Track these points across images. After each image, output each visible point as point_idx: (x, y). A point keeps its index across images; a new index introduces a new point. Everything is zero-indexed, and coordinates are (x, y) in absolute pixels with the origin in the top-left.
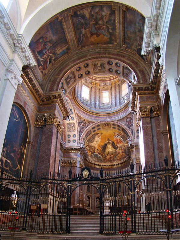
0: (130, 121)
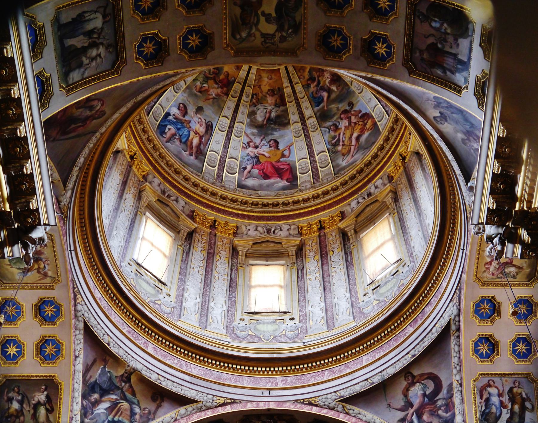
0: (432, 397)
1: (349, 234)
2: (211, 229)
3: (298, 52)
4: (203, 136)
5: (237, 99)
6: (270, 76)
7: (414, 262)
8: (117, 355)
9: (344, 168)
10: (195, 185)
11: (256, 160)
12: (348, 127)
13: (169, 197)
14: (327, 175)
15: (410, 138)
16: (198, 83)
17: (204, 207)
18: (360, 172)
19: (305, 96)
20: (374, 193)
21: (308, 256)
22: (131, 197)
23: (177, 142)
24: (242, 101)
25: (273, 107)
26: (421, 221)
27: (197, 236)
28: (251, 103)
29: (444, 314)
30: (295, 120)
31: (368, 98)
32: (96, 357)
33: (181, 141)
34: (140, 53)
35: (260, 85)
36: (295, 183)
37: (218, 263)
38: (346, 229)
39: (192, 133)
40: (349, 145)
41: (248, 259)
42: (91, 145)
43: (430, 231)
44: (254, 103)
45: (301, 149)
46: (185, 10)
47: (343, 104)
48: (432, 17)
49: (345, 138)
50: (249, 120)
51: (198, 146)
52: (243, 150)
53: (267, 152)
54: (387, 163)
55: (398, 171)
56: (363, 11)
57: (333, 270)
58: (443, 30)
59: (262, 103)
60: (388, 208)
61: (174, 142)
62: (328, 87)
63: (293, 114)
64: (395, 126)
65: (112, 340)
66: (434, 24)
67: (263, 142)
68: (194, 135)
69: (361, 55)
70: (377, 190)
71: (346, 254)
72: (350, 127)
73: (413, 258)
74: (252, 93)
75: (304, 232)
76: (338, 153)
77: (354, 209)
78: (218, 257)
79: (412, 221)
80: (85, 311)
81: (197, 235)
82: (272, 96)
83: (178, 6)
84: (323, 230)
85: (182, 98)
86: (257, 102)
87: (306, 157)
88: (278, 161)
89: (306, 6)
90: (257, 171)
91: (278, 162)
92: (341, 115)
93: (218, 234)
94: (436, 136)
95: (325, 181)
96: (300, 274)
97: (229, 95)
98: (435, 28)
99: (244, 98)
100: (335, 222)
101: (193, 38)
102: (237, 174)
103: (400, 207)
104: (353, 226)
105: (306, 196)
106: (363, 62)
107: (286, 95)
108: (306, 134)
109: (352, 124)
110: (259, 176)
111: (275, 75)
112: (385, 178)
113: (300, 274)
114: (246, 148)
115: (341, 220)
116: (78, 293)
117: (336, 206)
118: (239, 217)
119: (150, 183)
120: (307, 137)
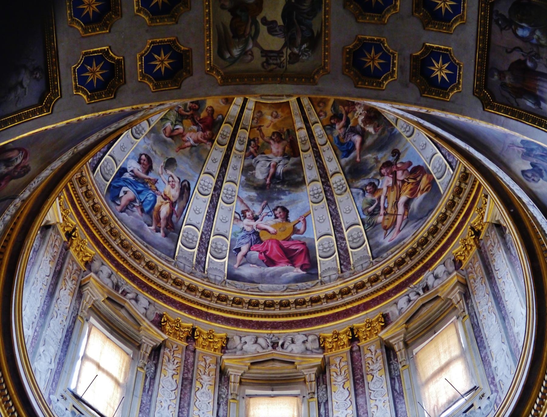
1: (396, 348)
2: (187, 342)
3: (316, 77)
5: (226, 146)
6: (274, 113)
7: (497, 391)
9: (386, 249)
10: (164, 275)
13: (124, 293)
14: (362, 258)
15: (486, 203)
16: (168, 124)
17: (177, 309)
18: (412, 254)
19: (327, 142)
20: (433, 287)
21: (334, 383)
22: (67, 295)
23: (138, 212)
24: (233, 150)
25: (279, 158)
26: (505, 328)
27: (166, 353)
28: (247, 153)
30: (313, 178)
33: (142, 211)
34: (82, 80)
35: (260, 126)
36: (313, 272)
37: (198, 394)
38: (391, 341)
39: (159, 199)
40: (394, 215)
41: (243, 387)
42: (8, 218)
43: (520, 344)
44: (251, 153)
45: (321, 221)
46: (150, 16)
47: (384, 153)
48: (517, 22)
50: (243, 178)
51: (169, 218)
52: (235, 222)
53: (272, 226)
54: (453, 241)
55: (468, 252)
56: (413, 14)
57: (373, 403)
58: (534, 41)
59: (264, 153)
60: (455, 308)
61: (133, 211)
62: (361, 128)
63: (310, 168)
64: (463, 185)
66: (520, 32)
67: (266, 211)
68: (163, 200)
69: (410, 81)
70: (437, 281)
71: (392, 379)
72: (395, 187)
73: (495, 386)
74: (249, 138)
75: (328, 345)
76: (377, 226)
77: (403, 311)
78: (198, 385)
79: (492, 328)
81: (167, 351)
82: (279, 142)
83: (139, 11)
84: (356, 342)
85: (144, 146)
86: (255, 151)
87: (329, 232)
88: (288, 239)
89: (327, 9)
90: (257, 254)
91: (288, 240)
92: (381, 169)
93: (199, 349)
94: (526, 199)
95: (359, 268)
96: (322, 411)
97: (214, 141)
98: (522, 38)
99: (237, 145)
100: (375, 330)
101: (160, 58)
102: (226, 259)
103: (472, 306)
104: (403, 335)
105: (330, 292)
106: (414, 91)
108: (329, 197)
109: (398, 183)
110: (260, 262)
111: (283, 111)
112: (449, 262)
113: (322, 411)
114: (240, 220)
115: (383, 328)
117: (375, 306)
118: (230, 323)
119: (96, 273)
120: (331, 202)
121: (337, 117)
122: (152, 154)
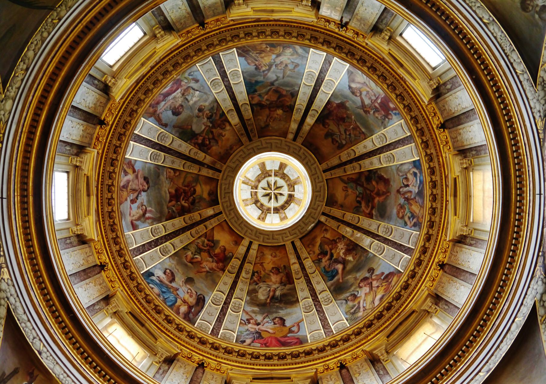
4: (193, 307)
5: (235, 275)
6: (274, 254)
8: (51, 371)
11: (257, 335)
12: (369, 292)
16: (189, 253)
24: (241, 277)
25: (277, 285)
28: (252, 281)
29: (526, 299)
31: (391, 255)
32: (18, 366)
35: (262, 263)
38: (374, 352)
44: (255, 281)
45: (312, 323)
49: (366, 303)
50: (248, 298)
59: (265, 282)
60: (429, 312)
62: (343, 258)
63: (302, 290)
64: (428, 152)
65: (45, 350)
80: (11, 295)
82: (277, 274)
85: (169, 263)
88: (285, 336)
90: (259, 345)
92: (359, 283)
99: (243, 274)
104: (384, 346)
107: (293, 272)
109: (374, 289)
111: (280, 252)
114: (245, 324)
116: (4, 265)
120: (320, 311)
121: (324, 253)
122: (175, 271)
